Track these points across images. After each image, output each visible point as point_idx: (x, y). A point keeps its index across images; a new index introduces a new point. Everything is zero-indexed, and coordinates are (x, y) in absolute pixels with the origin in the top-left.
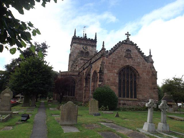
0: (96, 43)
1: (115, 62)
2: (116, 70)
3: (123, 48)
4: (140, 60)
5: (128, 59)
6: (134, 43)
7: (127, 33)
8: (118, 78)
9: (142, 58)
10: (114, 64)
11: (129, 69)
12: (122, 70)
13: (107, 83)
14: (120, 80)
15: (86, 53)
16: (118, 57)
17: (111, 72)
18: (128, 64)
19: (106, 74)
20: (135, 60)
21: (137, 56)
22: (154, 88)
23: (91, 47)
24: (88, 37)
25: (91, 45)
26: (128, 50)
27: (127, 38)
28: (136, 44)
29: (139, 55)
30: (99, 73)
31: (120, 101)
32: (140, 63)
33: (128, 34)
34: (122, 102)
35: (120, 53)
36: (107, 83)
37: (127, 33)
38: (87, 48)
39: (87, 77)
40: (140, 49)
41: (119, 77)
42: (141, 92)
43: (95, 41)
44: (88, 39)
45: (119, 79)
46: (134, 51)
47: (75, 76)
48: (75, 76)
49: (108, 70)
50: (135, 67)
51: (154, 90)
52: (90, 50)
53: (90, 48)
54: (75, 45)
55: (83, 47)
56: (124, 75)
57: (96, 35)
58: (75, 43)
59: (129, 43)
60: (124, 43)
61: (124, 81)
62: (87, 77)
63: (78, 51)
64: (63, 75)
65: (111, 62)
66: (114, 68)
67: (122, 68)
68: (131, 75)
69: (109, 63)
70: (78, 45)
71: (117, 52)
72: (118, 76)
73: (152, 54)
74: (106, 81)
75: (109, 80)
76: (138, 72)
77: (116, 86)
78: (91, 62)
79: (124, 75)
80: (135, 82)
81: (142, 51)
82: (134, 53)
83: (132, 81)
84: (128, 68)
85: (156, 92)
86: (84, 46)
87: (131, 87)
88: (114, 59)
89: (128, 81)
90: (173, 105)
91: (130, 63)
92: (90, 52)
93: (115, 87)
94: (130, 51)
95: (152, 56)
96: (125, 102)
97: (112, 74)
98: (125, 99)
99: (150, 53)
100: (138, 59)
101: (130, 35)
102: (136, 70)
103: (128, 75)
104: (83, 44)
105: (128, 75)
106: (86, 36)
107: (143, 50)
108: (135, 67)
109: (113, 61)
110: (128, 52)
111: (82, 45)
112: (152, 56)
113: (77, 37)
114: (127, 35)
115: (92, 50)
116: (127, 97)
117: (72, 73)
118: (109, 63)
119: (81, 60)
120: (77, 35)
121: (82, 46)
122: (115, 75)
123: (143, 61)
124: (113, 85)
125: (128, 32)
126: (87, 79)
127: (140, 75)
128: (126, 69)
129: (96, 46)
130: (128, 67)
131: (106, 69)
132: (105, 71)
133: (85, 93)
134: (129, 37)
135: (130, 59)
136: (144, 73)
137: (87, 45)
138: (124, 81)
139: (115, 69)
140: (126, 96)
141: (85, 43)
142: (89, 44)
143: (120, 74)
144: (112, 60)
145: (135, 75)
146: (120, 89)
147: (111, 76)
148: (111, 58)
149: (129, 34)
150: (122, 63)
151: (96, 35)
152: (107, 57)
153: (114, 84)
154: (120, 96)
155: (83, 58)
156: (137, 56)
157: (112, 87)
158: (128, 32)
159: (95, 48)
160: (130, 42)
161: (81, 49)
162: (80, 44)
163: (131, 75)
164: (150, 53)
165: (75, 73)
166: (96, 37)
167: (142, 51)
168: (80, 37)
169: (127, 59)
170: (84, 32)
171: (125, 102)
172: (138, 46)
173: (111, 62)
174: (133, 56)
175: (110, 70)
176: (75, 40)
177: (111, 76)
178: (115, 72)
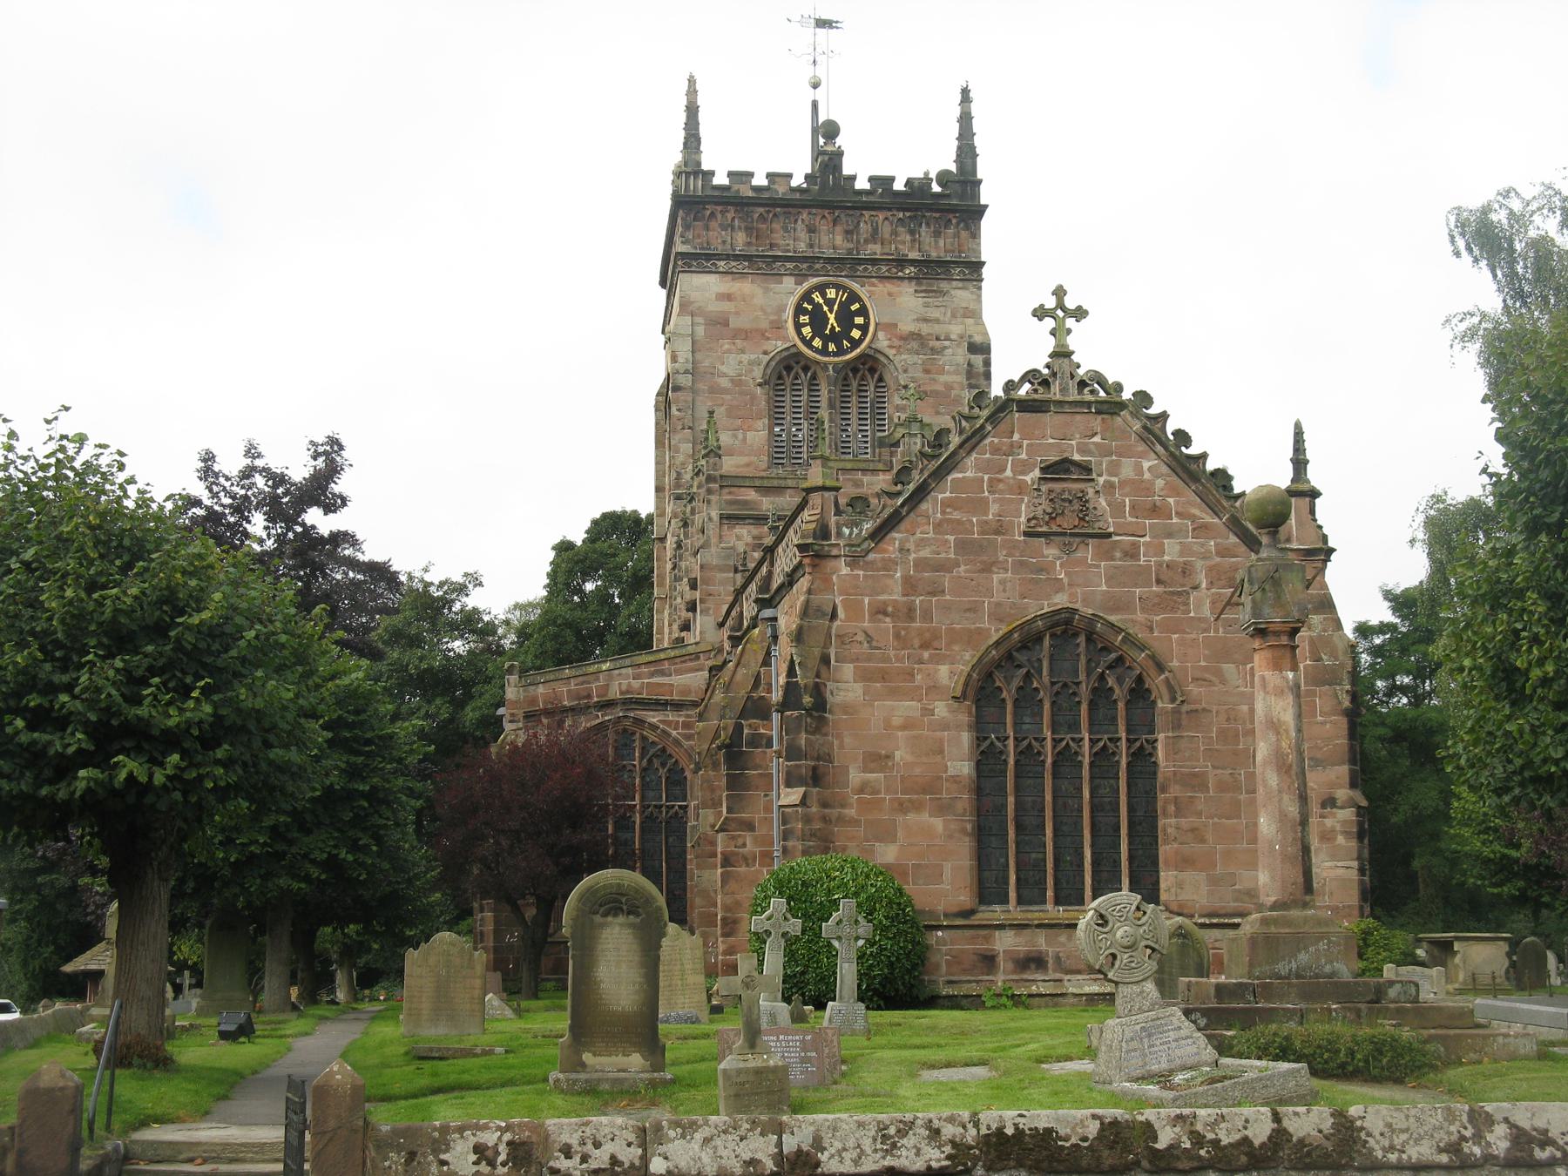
0: (975, 235)
1: (933, 594)
2: (944, 670)
3: (1012, 449)
4: (1188, 543)
5: (1067, 549)
6: (1119, 387)
7: (1051, 303)
8: (966, 738)
9: (1209, 518)
10: (927, 615)
11: (1082, 639)
12: (1009, 657)
13: (861, 790)
14: (987, 759)
15: (853, 367)
16: (962, 546)
17: (894, 693)
18: (1061, 600)
19: (847, 708)
20: (1132, 553)
21: (1155, 510)
22: (1323, 806)
23: (908, 289)
24: (860, 167)
25: (902, 262)
26: (1058, 469)
27: (1050, 344)
28: (1144, 398)
29: (1182, 501)
30: (783, 706)
31: (987, 939)
32: (1186, 570)
33: (1064, 309)
34: (1005, 942)
35: (981, 506)
36: (861, 790)
37: (1051, 303)
38: (863, 312)
39: (739, 728)
40: (1183, 437)
41: (980, 728)
42: (1203, 841)
43: (951, 204)
44: (862, 184)
45: (980, 740)
46: (1127, 470)
47: (678, 706)
48: (678, 706)
49: (864, 676)
50: (1133, 621)
51: (1329, 822)
52: (907, 326)
53: (894, 307)
54: (703, 286)
55: (807, 297)
56: (1026, 699)
57: (965, 120)
58: (699, 260)
59: (1073, 396)
60: (1027, 406)
61: (1028, 755)
62: (739, 728)
63: (741, 365)
64: (547, 713)
65: (895, 595)
66: (926, 655)
67: (997, 643)
68: (1101, 694)
69: (880, 611)
70: (746, 287)
71: (946, 504)
72: (964, 718)
73: (1315, 477)
74: (855, 776)
75: (878, 760)
76: (1161, 668)
77: (942, 809)
78: (764, 587)
79: (1026, 699)
80: (1142, 758)
81: (1204, 456)
82: (1123, 483)
83: (1103, 757)
84: (1064, 626)
85: (1341, 839)
86: (821, 289)
87: (1103, 808)
88: (921, 564)
89: (1065, 758)
90: (1456, 946)
91: (1080, 584)
92: (903, 365)
93: (938, 824)
94: (1086, 468)
95: (1314, 494)
96: (1041, 942)
97: (907, 708)
98: (1034, 914)
99: (1300, 463)
100: (1170, 535)
101: (1080, 313)
102: (1142, 647)
103: (1064, 692)
104: (804, 264)
105: (1064, 692)
106: (828, 162)
107: (1215, 446)
108: (1140, 616)
109: (910, 586)
110: (1057, 486)
111: (789, 282)
112: (1314, 494)
113: (721, 179)
114: (1049, 323)
115: (925, 329)
116: (1058, 901)
117: (636, 684)
118: (880, 611)
119: (729, 519)
120: (719, 162)
121: (789, 291)
122: (941, 709)
123: (1223, 552)
124: (917, 807)
125: (1060, 293)
126: (736, 754)
127: (1194, 689)
128: (1047, 641)
129: (973, 269)
130: (1068, 622)
131: (848, 670)
132: (846, 689)
133: (732, 885)
134: (1072, 342)
135: (1089, 552)
136: (1229, 668)
137: (851, 264)
138: (1028, 755)
139: (938, 660)
140: (1050, 893)
141: (833, 241)
142: (874, 249)
143: (981, 693)
144: (907, 580)
145: (1140, 693)
146: (985, 834)
147: (904, 727)
148: (889, 565)
149: (1070, 303)
150: (1008, 597)
151: (965, 120)
152: (855, 560)
153: (925, 790)
154: (988, 890)
155: (751, 495)
156: (1155, 510)
157: (911, 817)
158: (1060, 293)
159: (961, 296)
160: (1082, 384)
161: (778, 326)
162: (763, 264)
163: (1101, 694)
164: (1300, 463)
165: (677, 680)
166: (967, 151)
167: (1204, 456)
168: (760, 180)
169: (1051, 551)
170: (815, 86)
171: (1041, 942)
172: (1164, 416)
173: (895, 595)
174: (1118, 509)
175: (884, 676)
176: (714, 221)
177: (896, 721)
178: (934, 689)
